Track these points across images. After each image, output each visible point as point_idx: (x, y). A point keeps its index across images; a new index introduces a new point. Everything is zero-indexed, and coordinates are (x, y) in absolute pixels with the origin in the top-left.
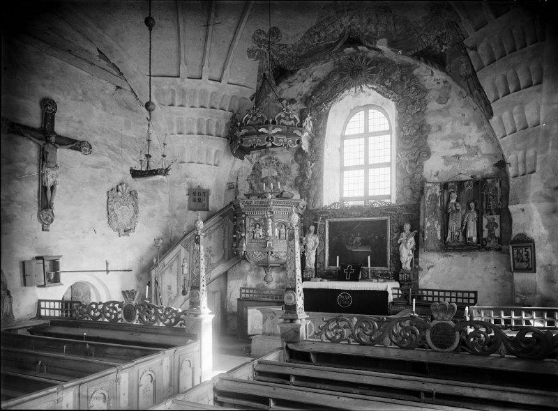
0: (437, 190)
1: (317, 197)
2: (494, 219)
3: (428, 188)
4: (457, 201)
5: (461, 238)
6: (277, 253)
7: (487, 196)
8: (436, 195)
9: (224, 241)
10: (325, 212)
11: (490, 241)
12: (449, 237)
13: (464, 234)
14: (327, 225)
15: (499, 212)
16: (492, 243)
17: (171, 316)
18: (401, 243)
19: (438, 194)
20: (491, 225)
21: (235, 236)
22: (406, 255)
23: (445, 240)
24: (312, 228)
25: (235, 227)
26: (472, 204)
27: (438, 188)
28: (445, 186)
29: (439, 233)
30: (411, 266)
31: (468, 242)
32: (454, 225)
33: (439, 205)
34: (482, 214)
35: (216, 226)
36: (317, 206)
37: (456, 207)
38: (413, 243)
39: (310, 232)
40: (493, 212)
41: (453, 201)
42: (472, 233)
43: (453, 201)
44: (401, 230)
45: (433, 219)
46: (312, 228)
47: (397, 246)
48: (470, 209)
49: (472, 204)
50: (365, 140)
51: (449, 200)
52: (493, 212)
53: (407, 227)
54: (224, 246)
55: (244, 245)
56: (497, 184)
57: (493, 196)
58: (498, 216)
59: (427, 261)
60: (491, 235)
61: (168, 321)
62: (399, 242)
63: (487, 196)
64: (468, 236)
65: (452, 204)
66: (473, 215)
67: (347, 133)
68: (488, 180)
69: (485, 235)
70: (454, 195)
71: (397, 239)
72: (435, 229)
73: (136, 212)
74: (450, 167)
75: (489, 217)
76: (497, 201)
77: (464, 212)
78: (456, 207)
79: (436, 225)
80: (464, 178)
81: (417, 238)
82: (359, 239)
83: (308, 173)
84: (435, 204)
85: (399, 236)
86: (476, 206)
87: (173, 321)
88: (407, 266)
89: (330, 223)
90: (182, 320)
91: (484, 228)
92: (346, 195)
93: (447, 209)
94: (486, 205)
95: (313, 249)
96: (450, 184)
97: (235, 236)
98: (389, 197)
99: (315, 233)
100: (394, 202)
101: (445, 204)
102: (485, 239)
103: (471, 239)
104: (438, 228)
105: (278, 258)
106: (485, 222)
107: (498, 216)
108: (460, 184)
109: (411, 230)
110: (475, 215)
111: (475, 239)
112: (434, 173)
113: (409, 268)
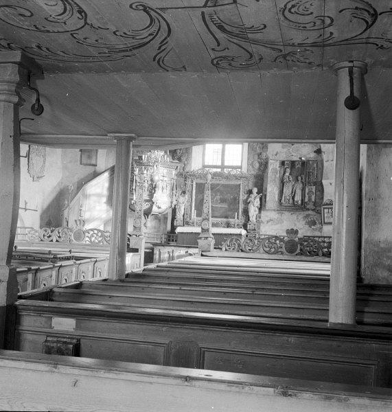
0: (278, 164)
4: (290, 174)
5: (291, 200)
10: (193, 175)
12: (283, 199)
13: (293, 198)
14: (194, 185)
15: (315, 184)
16: (310, 206)
19: (279, 169)
20: (310, 192)
22: (253, 211)
26: (300, 178)
27: (278, 165)
28: (283, 163)
29: (277, 197)
30: (256, 219)
32: (287, 191)
36: (187, 170)
38: (259, 202)
41: (287, 174)
42: (298, 198)
43: (287, 174)
44: (250, 192)
47: (247, 203)
49: (300, 178)
51: (284, 173)
53: (255, 190)
56: (315, 165)
59: (267, 216)
60: (310, 199)
64: (296, 199)
66: (299, 187)
69: (306, 200)
70: (288, 170)
71: (247, 199)
73: (44, 162)
74: (285, 150)
80: (295, 159)
81: (261, 199)
82: (218, 197)
85: (249, 197)
88: (253, 219)
92: (206, 164)
96: (286, 162)
98: (241, 167)
100: (244, 170)
103: (297, 202)
104: (276, 192)
105: (159, 208)
108: (293, 163)
109: (258, 193)
110: (301, 185)
111: (300, 202)
112: (275, 153)
113: (255, 221)
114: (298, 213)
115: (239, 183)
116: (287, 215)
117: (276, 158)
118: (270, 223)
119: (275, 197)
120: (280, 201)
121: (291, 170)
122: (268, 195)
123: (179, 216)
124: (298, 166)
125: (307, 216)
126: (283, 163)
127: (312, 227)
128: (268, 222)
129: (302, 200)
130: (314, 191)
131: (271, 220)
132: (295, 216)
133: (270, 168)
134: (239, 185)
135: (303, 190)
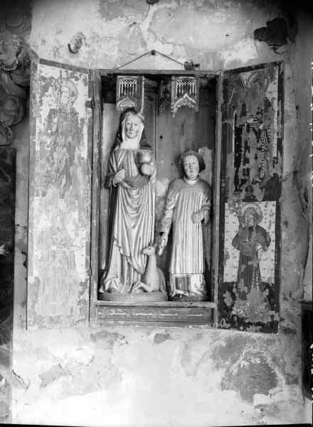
0: (80, 95)
2: (258, 217)
3: (48, 82)
4: (144, 145)
5: (154, 277)
7: (239, 131)
8: (74, 113)
11: (243, 297)
13: (165, 265)
15: (272, 190)
19: (83, 113)
20: (250, 230)
23: (100, 283)
26: (191, 162)
28: (106, 87)
29: (81, 258)
31: (175, 291)
33: (84, 153)
34: (224, 199)
37: (140, 165)
40: (258, 192)
41: (131, 143)
45: (62, 204)
48: (183, 175)
51: (117, 139)
52: (258, 192)
56: (273, 88)
57: (258, 133)
58: (272, 206)
60: (248, 271)
63: (239, 131)
64: (176, 270)
65: (128, 152)
66: (193, 200)
68: (245, 76)
69: (231, 272)
70: (136, 123)
72: (66, 243)
75: (245, 207)
76: (268, 151)
77: (162, 188)
78: (140, 165)
79: (70, 227)
84: (71, 149)
86: (202, 167)
91: (228, 245)
93: (111, 173)
94: (237, 164)
96: (122, 82)
101: (104, 160)
102: (228, 287)
104: (79, 235)
106: (232, 225)
107: (272, 206)
108: (158, 84)
110: (201, 197)
111: (197, 284)
114: (186, 333)
116: (138, 339)
117: (81, 60)
118: (56, 387)
119: (71, 263)
120: (101, 275)
121: (148, 122)
122: (36, 253)
124: (183, 100)
125: (231, 349)
126: (106, 87)
127: (260, 399)
128: (46, 381)
129: (207, 275)
130: (268, 224)
131: (61, 371)
132: (173, 348)
133: (43, 107)
135: (212, 224)
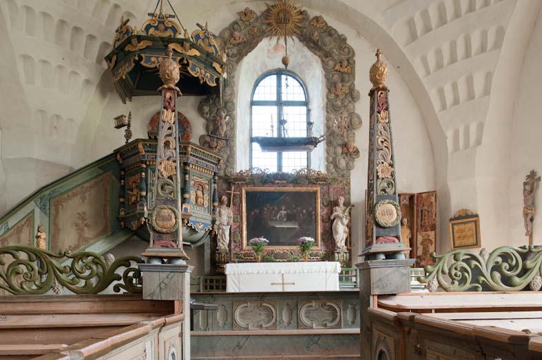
1: (231, 159)
6: (195, 223)
9: (105, 206)
10: (241, 179)
17: (87, 273)
18: (334, 219)
21: (122, 200)
24: (225, 198)
25: (123, 187)
35: (93, 182)
39: (221, 202)
46: (225, 198)
50: (285, 105)
54: (105, 214)
55: (145, 209)
61: (82, 283)
62: (332, 218)
67: (255, 99)
83: (222, 129)
87: (94, 281)
89: (247, 193)
90: (119, 279)
95: (228, 225)
97: (122, 200)
99: (228, 206)
115: (314, 189)
123: (223, 244)
134: (315, 193)
